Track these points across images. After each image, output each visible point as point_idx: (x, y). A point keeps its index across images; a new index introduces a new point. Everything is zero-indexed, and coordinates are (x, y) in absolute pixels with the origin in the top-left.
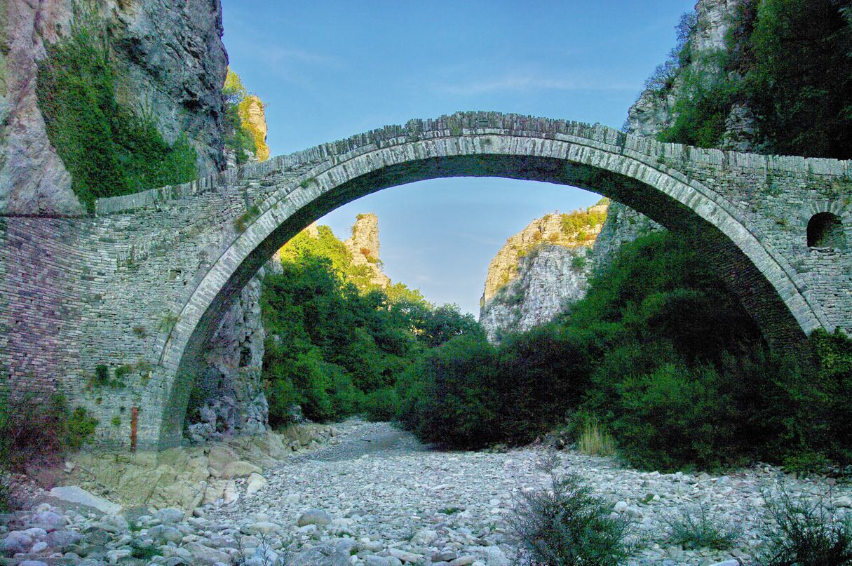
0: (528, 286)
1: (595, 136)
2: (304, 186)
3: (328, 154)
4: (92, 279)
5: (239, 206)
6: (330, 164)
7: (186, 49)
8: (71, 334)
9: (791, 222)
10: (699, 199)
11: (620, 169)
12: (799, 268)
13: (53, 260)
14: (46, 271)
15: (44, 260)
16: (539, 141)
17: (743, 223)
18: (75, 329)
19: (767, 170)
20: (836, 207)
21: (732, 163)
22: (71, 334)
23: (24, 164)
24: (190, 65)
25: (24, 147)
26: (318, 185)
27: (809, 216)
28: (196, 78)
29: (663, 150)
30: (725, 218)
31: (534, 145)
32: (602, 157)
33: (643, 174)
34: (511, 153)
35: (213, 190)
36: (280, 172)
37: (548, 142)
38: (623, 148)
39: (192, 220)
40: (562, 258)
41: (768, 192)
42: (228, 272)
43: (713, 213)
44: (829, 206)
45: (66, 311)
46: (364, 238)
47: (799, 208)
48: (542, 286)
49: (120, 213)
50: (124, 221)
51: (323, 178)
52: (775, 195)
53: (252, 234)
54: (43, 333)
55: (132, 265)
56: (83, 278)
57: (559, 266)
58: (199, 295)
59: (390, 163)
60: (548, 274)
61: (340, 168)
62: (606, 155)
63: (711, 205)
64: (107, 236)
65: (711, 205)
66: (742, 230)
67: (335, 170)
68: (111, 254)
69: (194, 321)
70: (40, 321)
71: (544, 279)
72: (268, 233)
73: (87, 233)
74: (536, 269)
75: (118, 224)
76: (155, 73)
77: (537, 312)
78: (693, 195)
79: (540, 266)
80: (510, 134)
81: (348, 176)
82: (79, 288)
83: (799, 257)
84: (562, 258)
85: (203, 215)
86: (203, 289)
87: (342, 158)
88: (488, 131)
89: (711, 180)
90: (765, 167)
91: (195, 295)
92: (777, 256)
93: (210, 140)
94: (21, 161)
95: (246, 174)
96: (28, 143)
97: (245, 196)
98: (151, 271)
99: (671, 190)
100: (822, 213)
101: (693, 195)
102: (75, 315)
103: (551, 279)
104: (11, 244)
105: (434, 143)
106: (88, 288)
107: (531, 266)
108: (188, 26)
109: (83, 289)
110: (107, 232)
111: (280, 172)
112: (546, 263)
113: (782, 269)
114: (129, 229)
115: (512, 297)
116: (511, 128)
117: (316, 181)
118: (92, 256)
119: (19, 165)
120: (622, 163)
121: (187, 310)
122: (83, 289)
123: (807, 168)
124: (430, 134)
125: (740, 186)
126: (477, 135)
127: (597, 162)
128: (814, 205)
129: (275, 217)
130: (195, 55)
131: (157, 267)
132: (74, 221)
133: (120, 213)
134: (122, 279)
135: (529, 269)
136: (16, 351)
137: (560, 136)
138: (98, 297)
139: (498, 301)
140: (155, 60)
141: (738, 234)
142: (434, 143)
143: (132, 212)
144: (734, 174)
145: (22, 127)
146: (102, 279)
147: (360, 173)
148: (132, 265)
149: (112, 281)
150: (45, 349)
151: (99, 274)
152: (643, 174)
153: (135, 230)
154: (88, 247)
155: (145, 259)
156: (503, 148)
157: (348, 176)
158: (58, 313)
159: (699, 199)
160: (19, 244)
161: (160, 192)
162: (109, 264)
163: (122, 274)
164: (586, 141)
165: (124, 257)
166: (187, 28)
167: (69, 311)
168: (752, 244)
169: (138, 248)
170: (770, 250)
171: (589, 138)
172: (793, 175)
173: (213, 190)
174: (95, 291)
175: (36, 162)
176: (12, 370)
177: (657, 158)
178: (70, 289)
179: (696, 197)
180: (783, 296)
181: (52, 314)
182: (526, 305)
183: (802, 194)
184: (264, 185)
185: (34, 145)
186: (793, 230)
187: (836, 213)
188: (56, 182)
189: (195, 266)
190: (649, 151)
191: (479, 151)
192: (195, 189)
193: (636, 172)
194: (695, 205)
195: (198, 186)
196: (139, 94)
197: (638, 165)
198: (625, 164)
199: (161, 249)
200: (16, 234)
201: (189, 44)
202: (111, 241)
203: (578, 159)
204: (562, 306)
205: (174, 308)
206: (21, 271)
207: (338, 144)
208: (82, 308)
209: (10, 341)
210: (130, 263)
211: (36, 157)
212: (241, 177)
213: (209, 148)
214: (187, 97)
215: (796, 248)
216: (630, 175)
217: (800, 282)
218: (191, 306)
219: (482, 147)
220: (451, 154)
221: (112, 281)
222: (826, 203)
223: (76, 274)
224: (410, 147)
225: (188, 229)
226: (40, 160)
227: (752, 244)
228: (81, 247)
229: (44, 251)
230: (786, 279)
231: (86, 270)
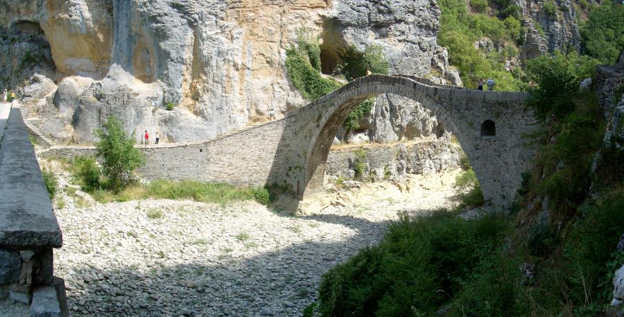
16: (391, 86)
27: (482, 122)
69: (310, 153)
89: (445, 104)
104: (255, 136)
160: (257, 136)
174: (287, 143)
186: (475, 129)
199: (302, 128)
202: (290, 126)
205: (306, 148)
207: (339, 90)
215: (476, 138)
217: (477, 155)
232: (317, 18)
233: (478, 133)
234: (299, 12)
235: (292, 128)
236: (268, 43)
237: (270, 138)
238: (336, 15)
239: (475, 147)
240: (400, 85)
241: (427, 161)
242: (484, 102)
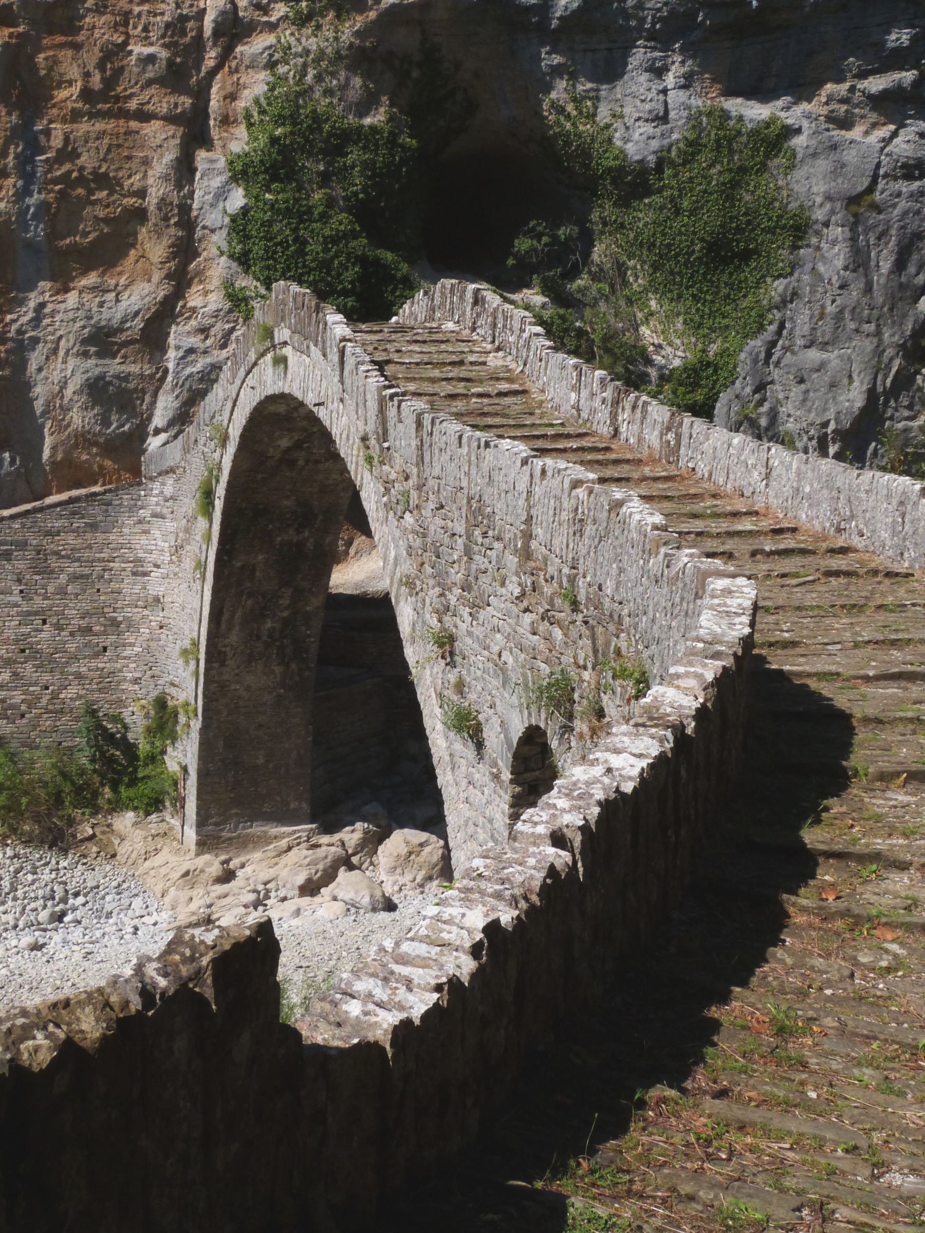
4: (145, 574)
8: (128, 652)
13: (78, 560)
14: (63, 578)
15: (53, 563)
18: (132, 645)
22: (128, 652)
25: (194, 341)
45: (115, 623)
54: (75, 658)
56: (134, 574)
70: (65, 643)
82: (130, 588)
96: (204, 331)
109: (137, 589)
110: (157, 504)
119: (188, 371)
122: (137, 589)
132: (108, 496)
136: (24, 685)
138: (157, 600)
150: (79, 676)
154: (137, 529)
158: (97, 628)
167: (121, 623)
176: (23, 707)
181: (87, 630)
185: (213, 331)
206: (16, 589)
208: (140, 616)
209: (15, 674)
223: (124, 570)
229: (57, 553)
231: (138, 561)
236: (134, 124)
237: (74, 568)
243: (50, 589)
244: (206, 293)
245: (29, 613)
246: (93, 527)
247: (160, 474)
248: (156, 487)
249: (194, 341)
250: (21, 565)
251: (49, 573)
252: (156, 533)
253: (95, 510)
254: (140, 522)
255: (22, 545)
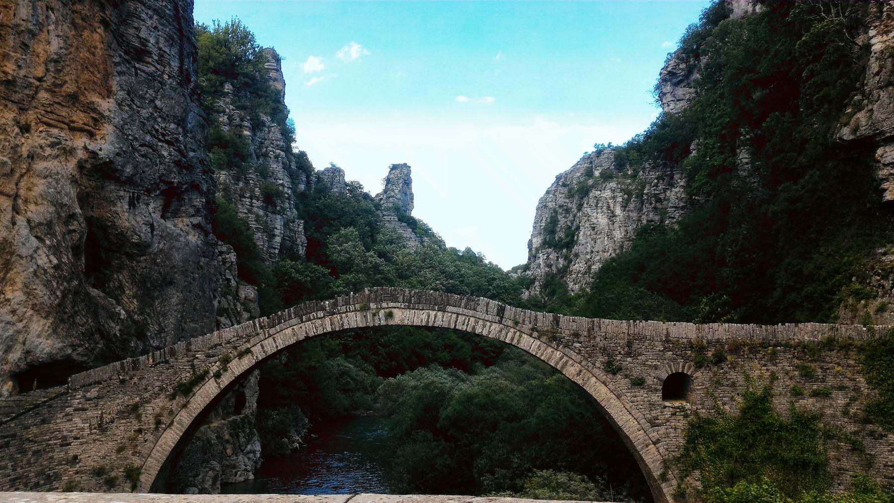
0: (578, 228)
1: (479, 308)
2: (241, 355)
3: (261, 328)
4: (69, 444)
5: (188, 375)
6: (262, 337)
7: (160, 140)
9: (649, 381)
10: (567, 362)
11: (499, 337)
12: (653, 423)
13: (36, 442)
14: (30, 453)
16: (432, 313)
17: (604, 383)
19: (628, 334)
20: (689, 368)
21: (596, 329)
23: (11, 332)
24: (165, 154)
25: (9, 318)
26: (253, 355)
27: (664, 376)
28: (173, 165)
29: (536, 319)
30: (589, 379)
31: (429, 317)
32: (484, 326)
33: (519, 341)
34: (410, 324)
35: (167, 362)
36: (221, 345)
37: (440, 314)
38: (502, 318)
39: (149, 388)
40: (614, 198)
41: (629, 354)
42: (181, 430)
43: (578, 374)
44: (683, 367)
45: (49, 477)
46: (396, 191)
47: (656, 369)
48: (593, 229)
49: (90, 385)
50: (93, 393)
51: (257, 350)
52: (635, 357)
53: (200, 398)
55: (102, 428)
56: (62, 446)
57: (612, 206)
58: (158, 451)
59: (311, 334)
60: (599, 216)
61: (271, 339)
62: (488, 324)
63: (577, 367)
64: (80, 406)
65: (577, 367)
66: (603, 389)
67: (266, 342)
68: (84, 421)
69: (154, 472)
71: (595, 221)
72: (213, 397)
73: (63, 408)
74: (587, 209)
75: (88, 395)
76: (130, 182)
77: (588, 257)
78: (561, 358)
79: (591, 206)
80: (409, 308)
81: (277, 347)
83: (654, 413)
84: (614, 198)
85: (158, 384)
86: (161, 446)
87: (272, 331)
88: (391, 305)
89: (578, 345)
90: (626, 332)
91: (154, 451)
92: (633, 412)
93: (192, 211)
94: (7, 330)
95: (193, 347)
96: (13, 312)
97: (193, 366)
98: (118, 432)
99: (542, 354)
100: (677, 374)
101: (561, 358)
102: (57, 477)
103: (602, 220)
105: (347, 316)
106: (66, 453)
107: (580, 207)
108: (160, 116)
110: (79, 403)
111: (221, 345)
112: (597, 203)
113: (639, 424)
114: (98, 398)
115: (561, 239)
116: (410, 302)
117: (251, 352)
118: (68, 425)
120: (501, 331)
121: (148, 463)
122: (62, 455)
123: (665, 332)
124: (344, 309)
125: (604, 350)
126: (382, 308)
127: (480, 330)
128: (670, 367)
129: (218, 383)
130: (169, 143)
131: (122, 428)
133: (90, 385)
134: (94, 440)
135: (579, 210)
137: (449, 308)
138: (75, 457)
139: (545, 244)
140: (129, 170)
141: (600, 390)
142: (347, 316)
143: (99, 383)
144: (598, 339)
145: (8, 300)
146: (77, 442)
147: (287, 344)
148: (102, 428)
149: (86, 443)
151: (76, 438)
152: (519, 341)
153: (103, 398)
155: (112, 422)
156: (402, 320)
157: (277, 347)
159: (567, 362)
161: (122, 365)
162: (83, 429)
163: (93, 436)
164: (471, 313)
165: (94, 422)
166: (159, 120)
168: (612, 401)
169: (105, 413)
170: (628, 408)
171: (474, 309)
172: (652, 339)
173: (167, 362)
175: (20, 325)
177: (530, 326)
178: (52, 458)
179: (564, 360)
180: (639, 448)
182: (576, 249)
183: (660, 356)
184: (208, 356)
187: (689, 373)
188: (39, 336)
189: (153, 426)
190: (524, 321)
191: (383, 323)
192: (151, 361)
193: (512, 339)
194: (563, 367)
195: (153, 357)
196: (115, 205)
197: (515, 333)
198: (504, 332)
200: (5, 437)
201: (163, 135)
202: (84, 410)
203: (465, 328)
204: (615, 250)
210: (100, 425)
211: (21, 321)
212: (189, 350)
213: (192, 219)
214: (163, 187)
215: (652, 405)
216: (507, 341)
217: (654, 435)
218: (152, 460)
219: (386, 320)
220: (361, 325)
221: (86, 443)
222: (681, 364)
223: (56, 444)
224: (327, 320)
225: (147, 395)
226: (25, 322)
227: (612, 401)
228: (58, 421)
229: (28, 439)
230: (642, 432)
231: (64, 438)
232: (81, 154)
233: (657, 397)
234: (55, 131)
235: (89, 413)
238: (111, 156)
239: (650, 421)
240: (460, 310)
241: (241, 457)
242: (668, 341)
243: (24, 462)
244: (13, 291)
245: (15, 479)
246: (44, 422)
247: (82, 387)
248: (79, 395)
249: (9, 318)
250: (12, 449)
251: (23, 452)
252: (77, 420)
253: (45, 411)
254: (67, 415)
255: (14, 436)
